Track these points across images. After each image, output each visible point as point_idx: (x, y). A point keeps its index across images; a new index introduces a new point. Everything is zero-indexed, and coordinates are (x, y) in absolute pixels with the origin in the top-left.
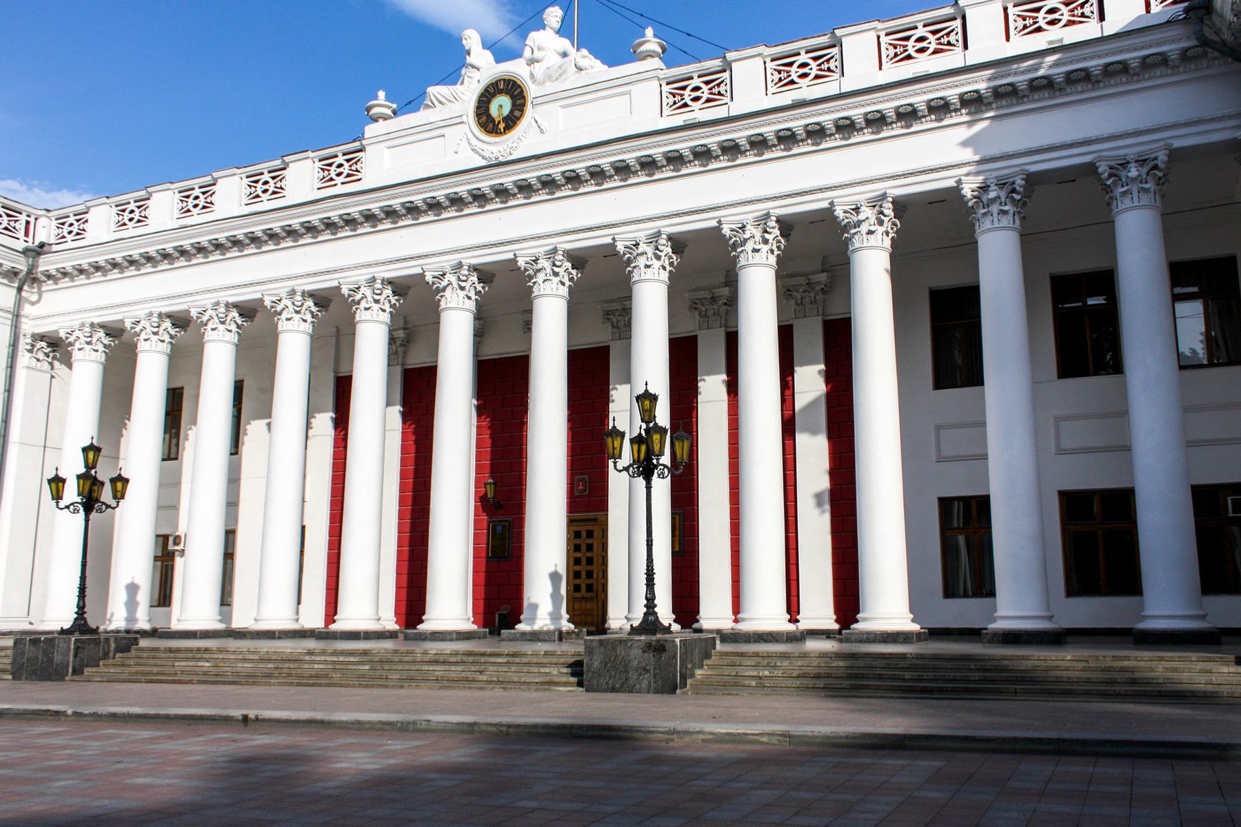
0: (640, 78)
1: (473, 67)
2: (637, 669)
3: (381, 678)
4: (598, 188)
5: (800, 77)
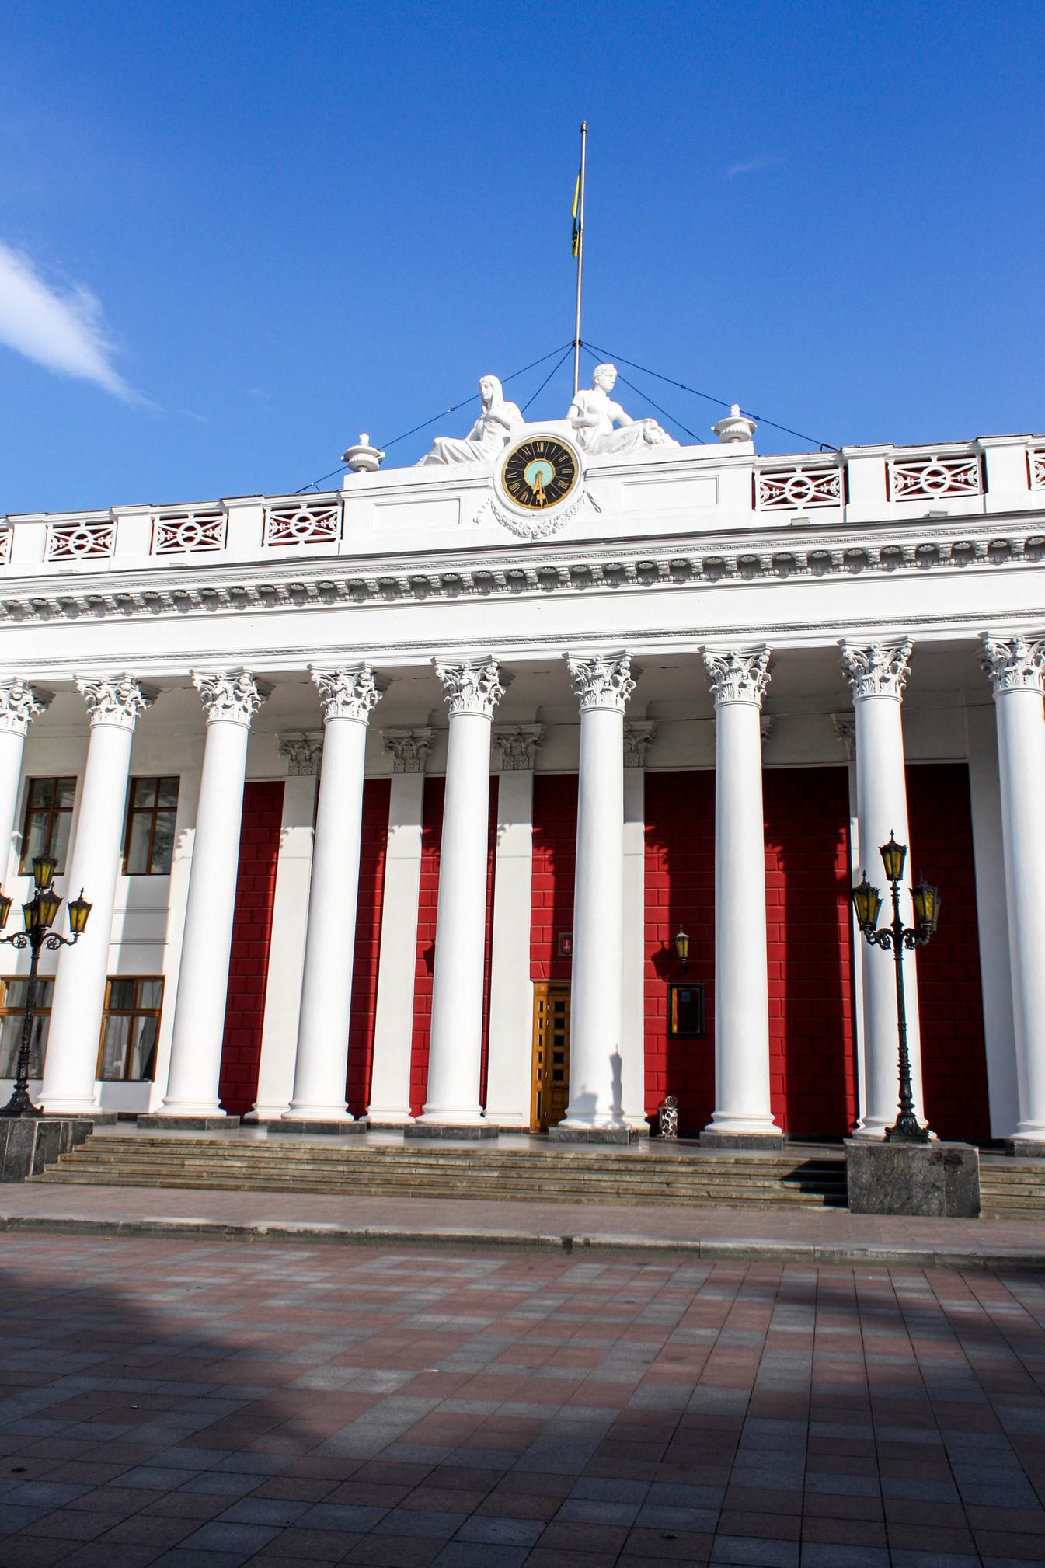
0: (733, 462)
1: (498, 421)
2: (922, 1185)
3: (531, 1188)
4: (676, 586)
5: (930, 485)
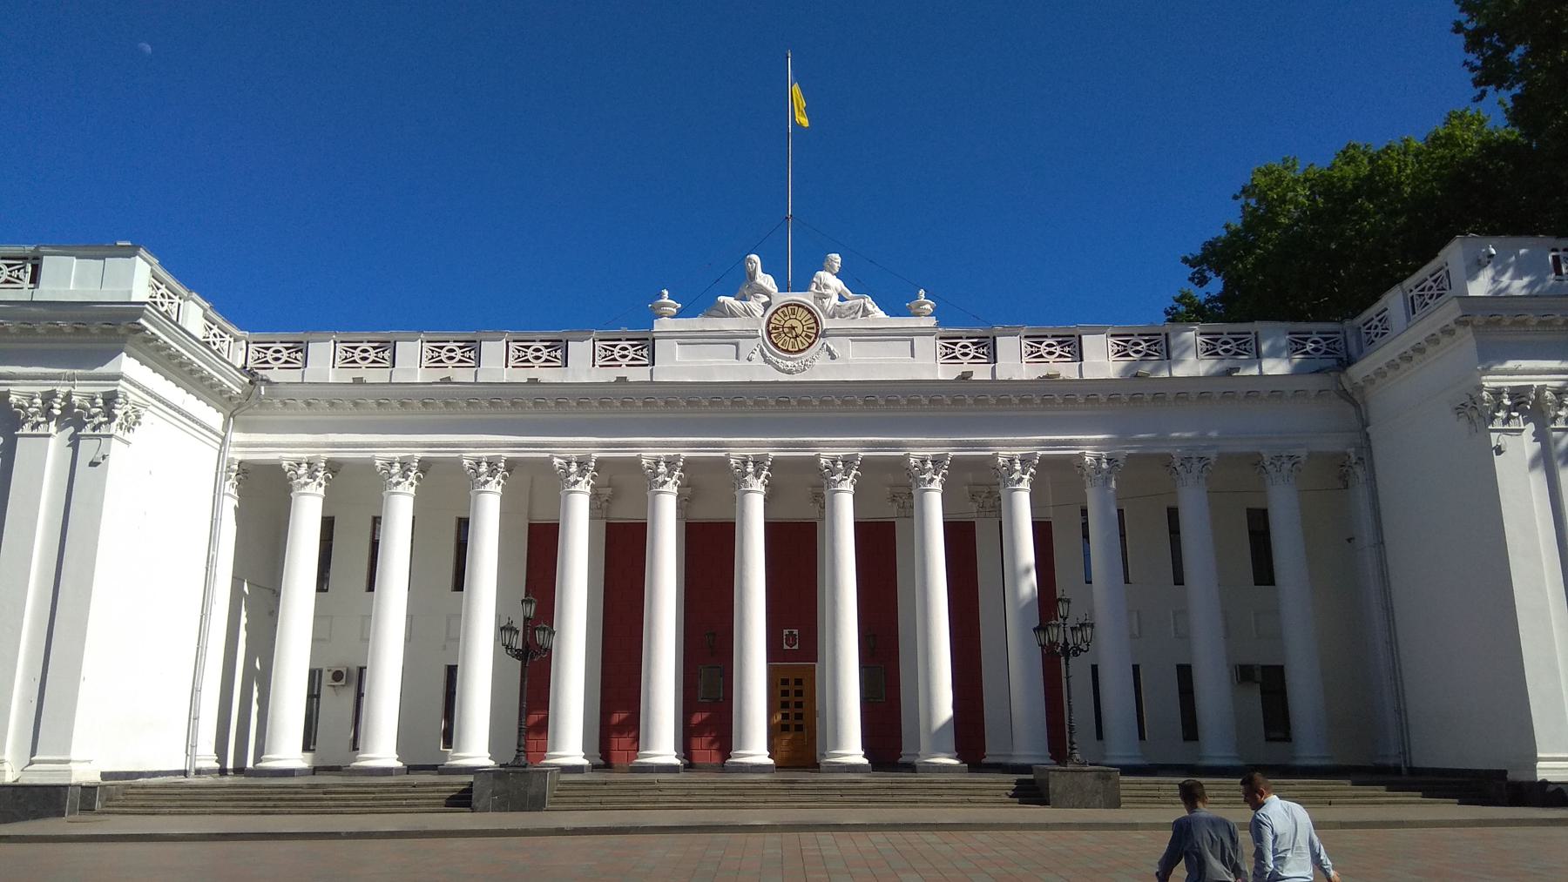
0: (924, 333)
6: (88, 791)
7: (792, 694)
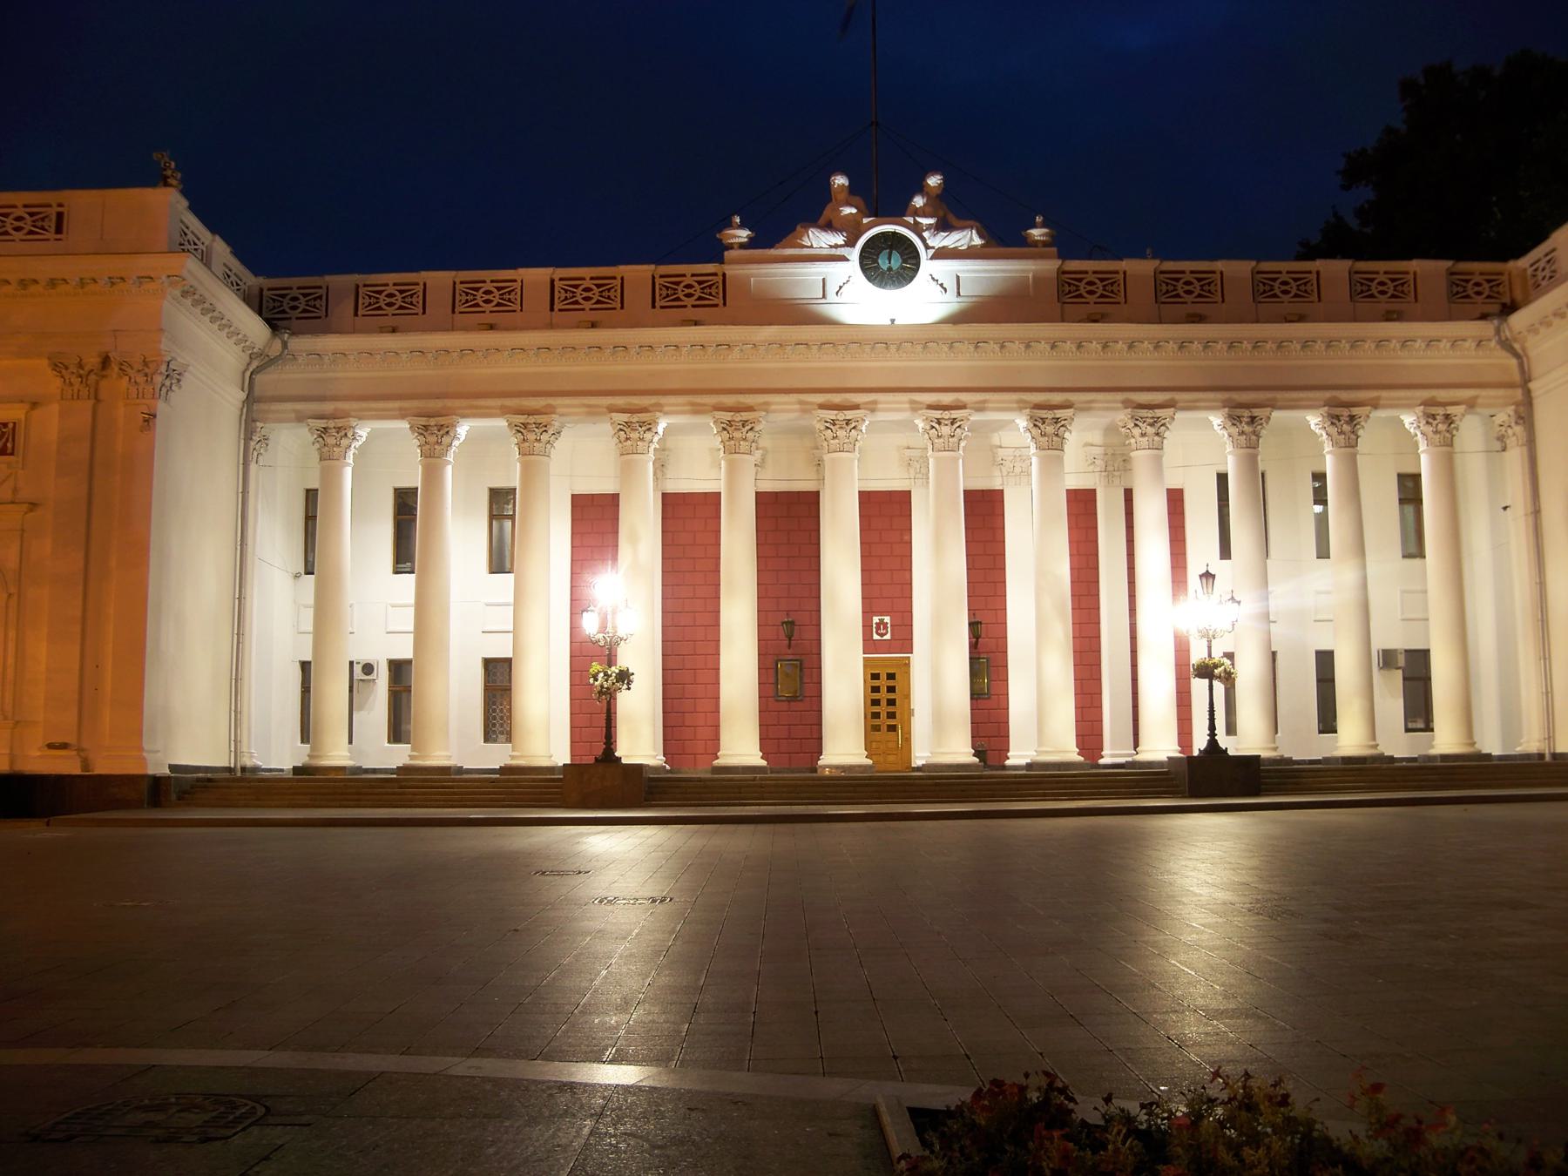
6: (157, 781)
7: (884, 690)
